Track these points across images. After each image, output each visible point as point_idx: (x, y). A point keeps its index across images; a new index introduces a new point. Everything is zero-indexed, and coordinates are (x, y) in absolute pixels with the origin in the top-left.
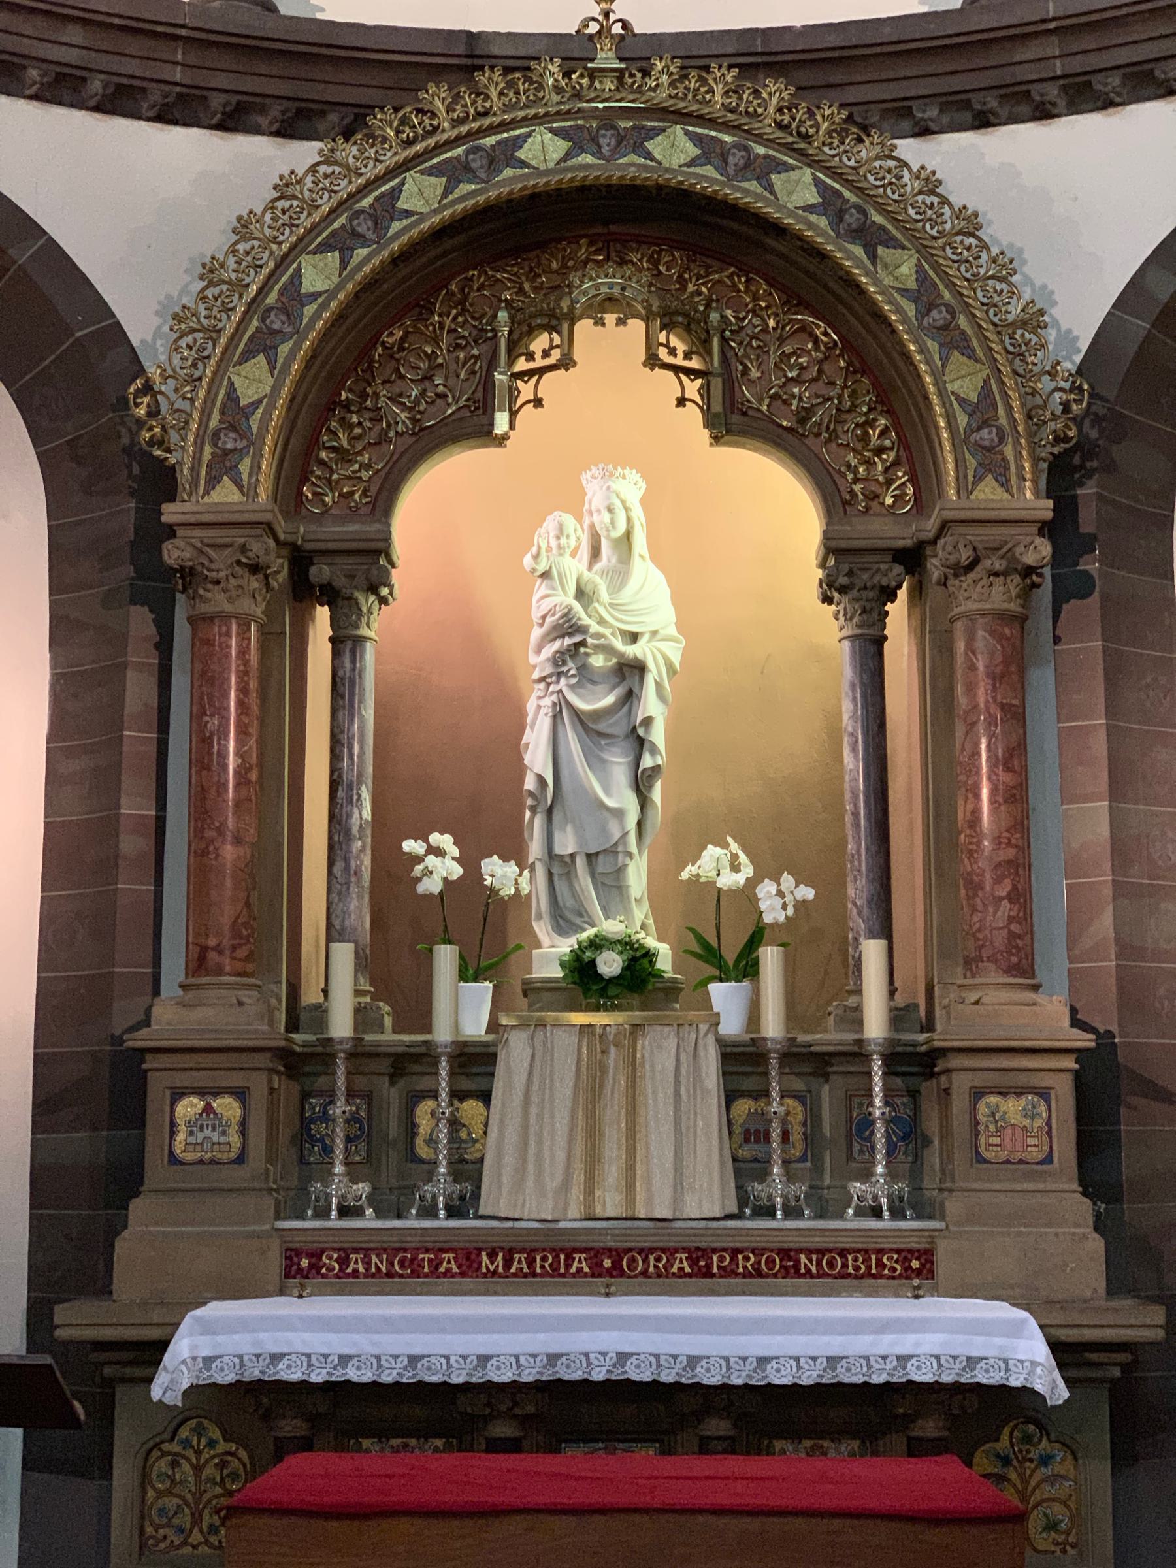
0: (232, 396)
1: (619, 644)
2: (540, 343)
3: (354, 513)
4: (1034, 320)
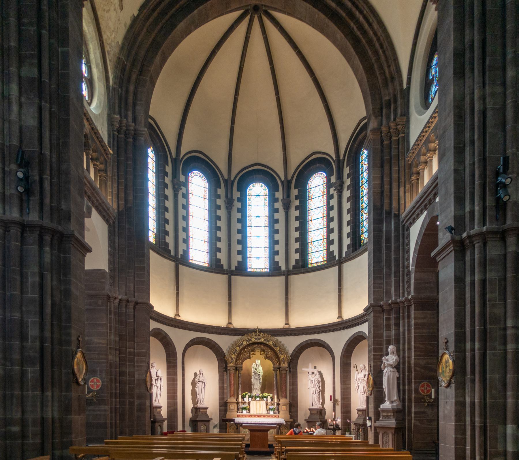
0: (232, 357)
1: (258, 373)
2: (253, 352)
3: (239, 364)
4: (287, 353)
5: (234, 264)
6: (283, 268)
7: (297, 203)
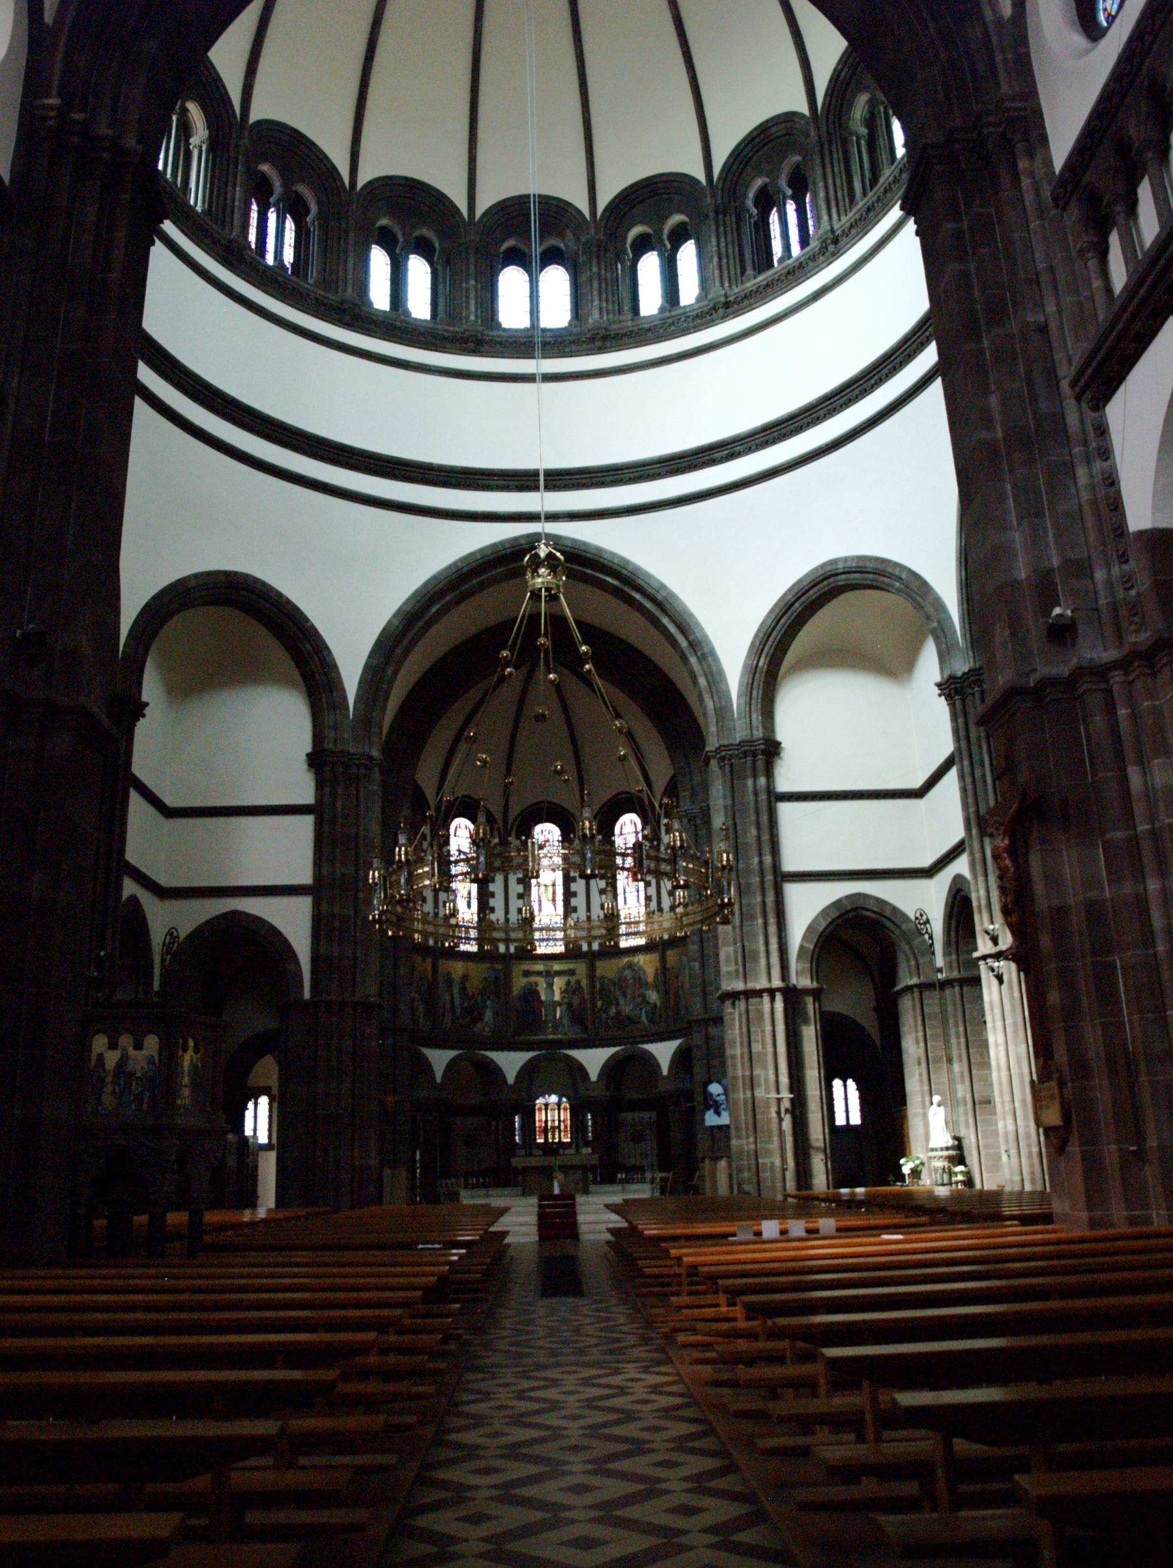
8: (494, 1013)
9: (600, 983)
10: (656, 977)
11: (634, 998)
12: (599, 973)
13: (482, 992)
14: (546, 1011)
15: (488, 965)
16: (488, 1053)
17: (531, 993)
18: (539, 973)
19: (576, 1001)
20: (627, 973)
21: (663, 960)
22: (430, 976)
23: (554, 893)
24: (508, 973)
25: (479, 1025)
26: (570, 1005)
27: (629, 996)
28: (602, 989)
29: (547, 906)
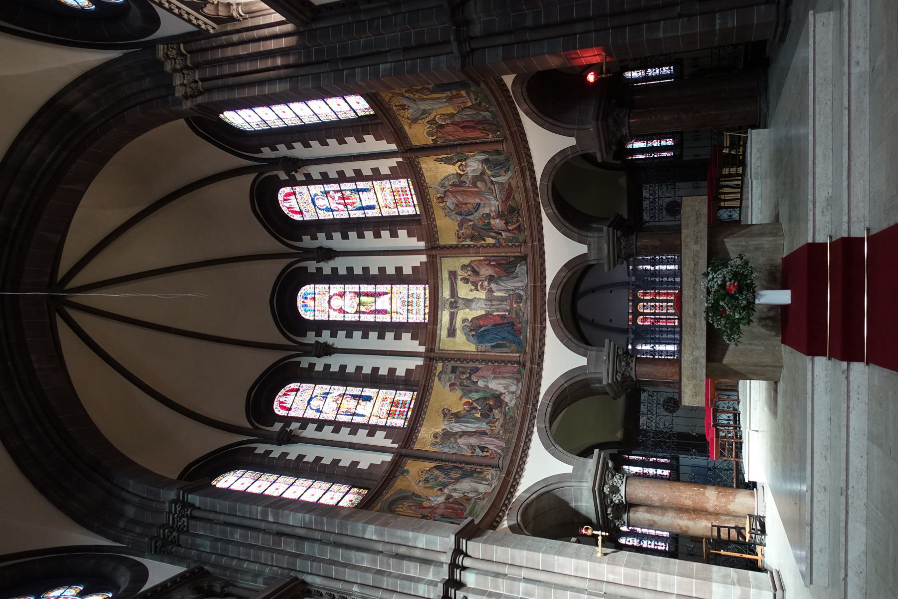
5: (415, 346)
6: (423, 258)
7: (321, 236)
8: (495, 378)
9: (465, 238)
10: (448, 161)
11: (479, 194)
12: (453, 242)
13: (466, 392)
14: (498, 310)
15: (436, 378)
16: (543, 390)
17: (477, 329)
18: (453, 317)
19: (486, 271)
20: (450, 202)
21: (425, 150)
22: (432, 465)
23: (367, 294)
24: (448, 357)
25: (507, 398)
26: (491, 279)
27: (478, 201)
28: (472, 238)
29: (382, 303)
